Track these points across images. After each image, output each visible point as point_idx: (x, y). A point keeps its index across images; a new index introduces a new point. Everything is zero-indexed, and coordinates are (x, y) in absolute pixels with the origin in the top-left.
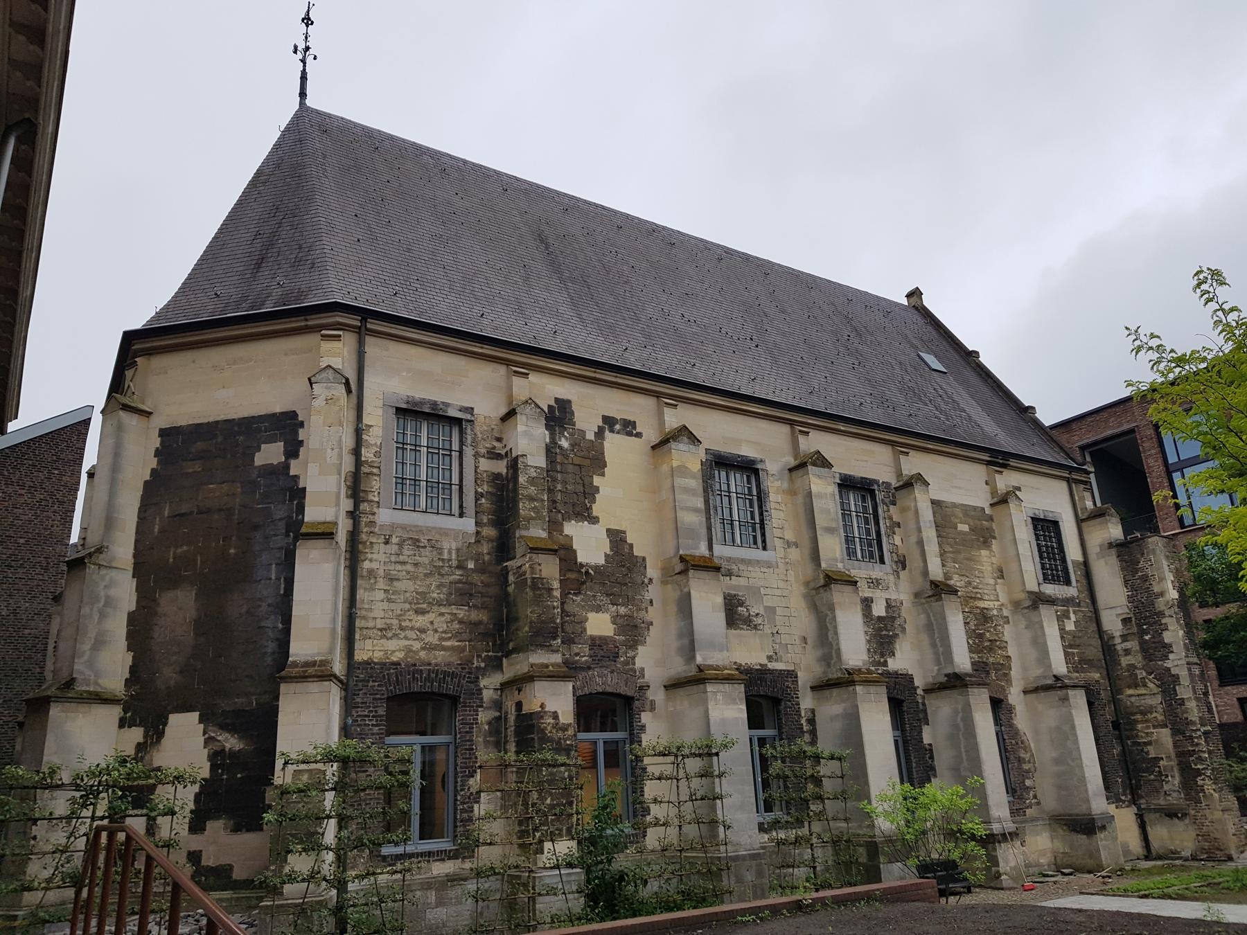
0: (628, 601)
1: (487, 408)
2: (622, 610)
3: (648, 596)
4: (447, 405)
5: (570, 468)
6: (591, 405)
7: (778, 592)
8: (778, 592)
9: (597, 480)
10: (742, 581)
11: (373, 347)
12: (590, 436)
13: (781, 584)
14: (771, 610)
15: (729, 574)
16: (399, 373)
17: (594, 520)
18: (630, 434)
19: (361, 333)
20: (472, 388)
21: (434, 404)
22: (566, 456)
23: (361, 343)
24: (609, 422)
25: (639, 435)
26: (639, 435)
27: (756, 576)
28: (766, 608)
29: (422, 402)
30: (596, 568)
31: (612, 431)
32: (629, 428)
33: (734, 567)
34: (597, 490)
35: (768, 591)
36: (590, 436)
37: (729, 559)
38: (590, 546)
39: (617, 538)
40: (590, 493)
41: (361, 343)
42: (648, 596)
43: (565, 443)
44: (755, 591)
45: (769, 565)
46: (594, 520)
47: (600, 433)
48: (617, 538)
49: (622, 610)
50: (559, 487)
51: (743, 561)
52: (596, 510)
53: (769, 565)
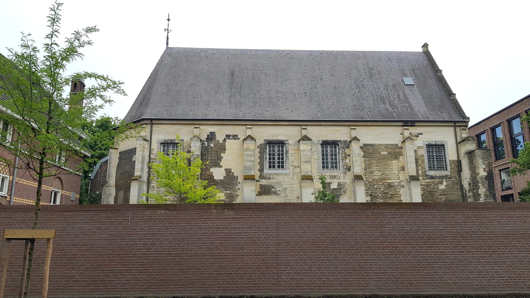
0: (231, 189)
1: (186, 138)
2: (228, 192)
3: (238, 187)
4: (175, 140)
5: (213, 152)
6: (221, 132)
7: (288, 183)
8: (288, 183)
9: (222, 155)
10: (274, 181)
11: (155, 127)
12: (221, 142)
13: (290, 180)
14: (286, 189)
15: (269, 179)
16: (162, 132)
17: (221, 167)
18: (235, 139)
19: (152, 124)
20: (182, 133)
21: (172, 140)
22: (212, 149)
23: (152, 127)
24: (228, 136)
25: (239, 139)
26: (239, 139)
27: (280, 178)
28: (283, 188)
29: (168, 140)
30: (220, 180)
31: (229, 139)
32: (235, 137)
33: (272, 176)
34: (222, 157)
35: (285, 183)
36: (221, 142)
37: (269, 174)
38: (218, 174)
39: (228, 171)
40: (220, 158)
41: (152, 127)
42: (238, 187)
43: (212, 145)
44: (279, 184)
45: (286, 174)
46: (221, 167)
47: (225, 140)
48: (228, 171)
49: (228, 192)
50: (209, 158)
51: (275, 174)
52: (221, 164)
53: (286, 174)
